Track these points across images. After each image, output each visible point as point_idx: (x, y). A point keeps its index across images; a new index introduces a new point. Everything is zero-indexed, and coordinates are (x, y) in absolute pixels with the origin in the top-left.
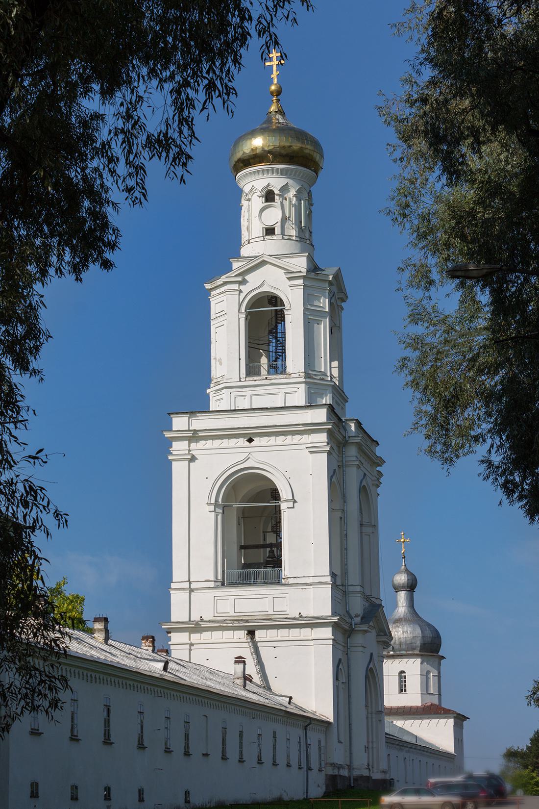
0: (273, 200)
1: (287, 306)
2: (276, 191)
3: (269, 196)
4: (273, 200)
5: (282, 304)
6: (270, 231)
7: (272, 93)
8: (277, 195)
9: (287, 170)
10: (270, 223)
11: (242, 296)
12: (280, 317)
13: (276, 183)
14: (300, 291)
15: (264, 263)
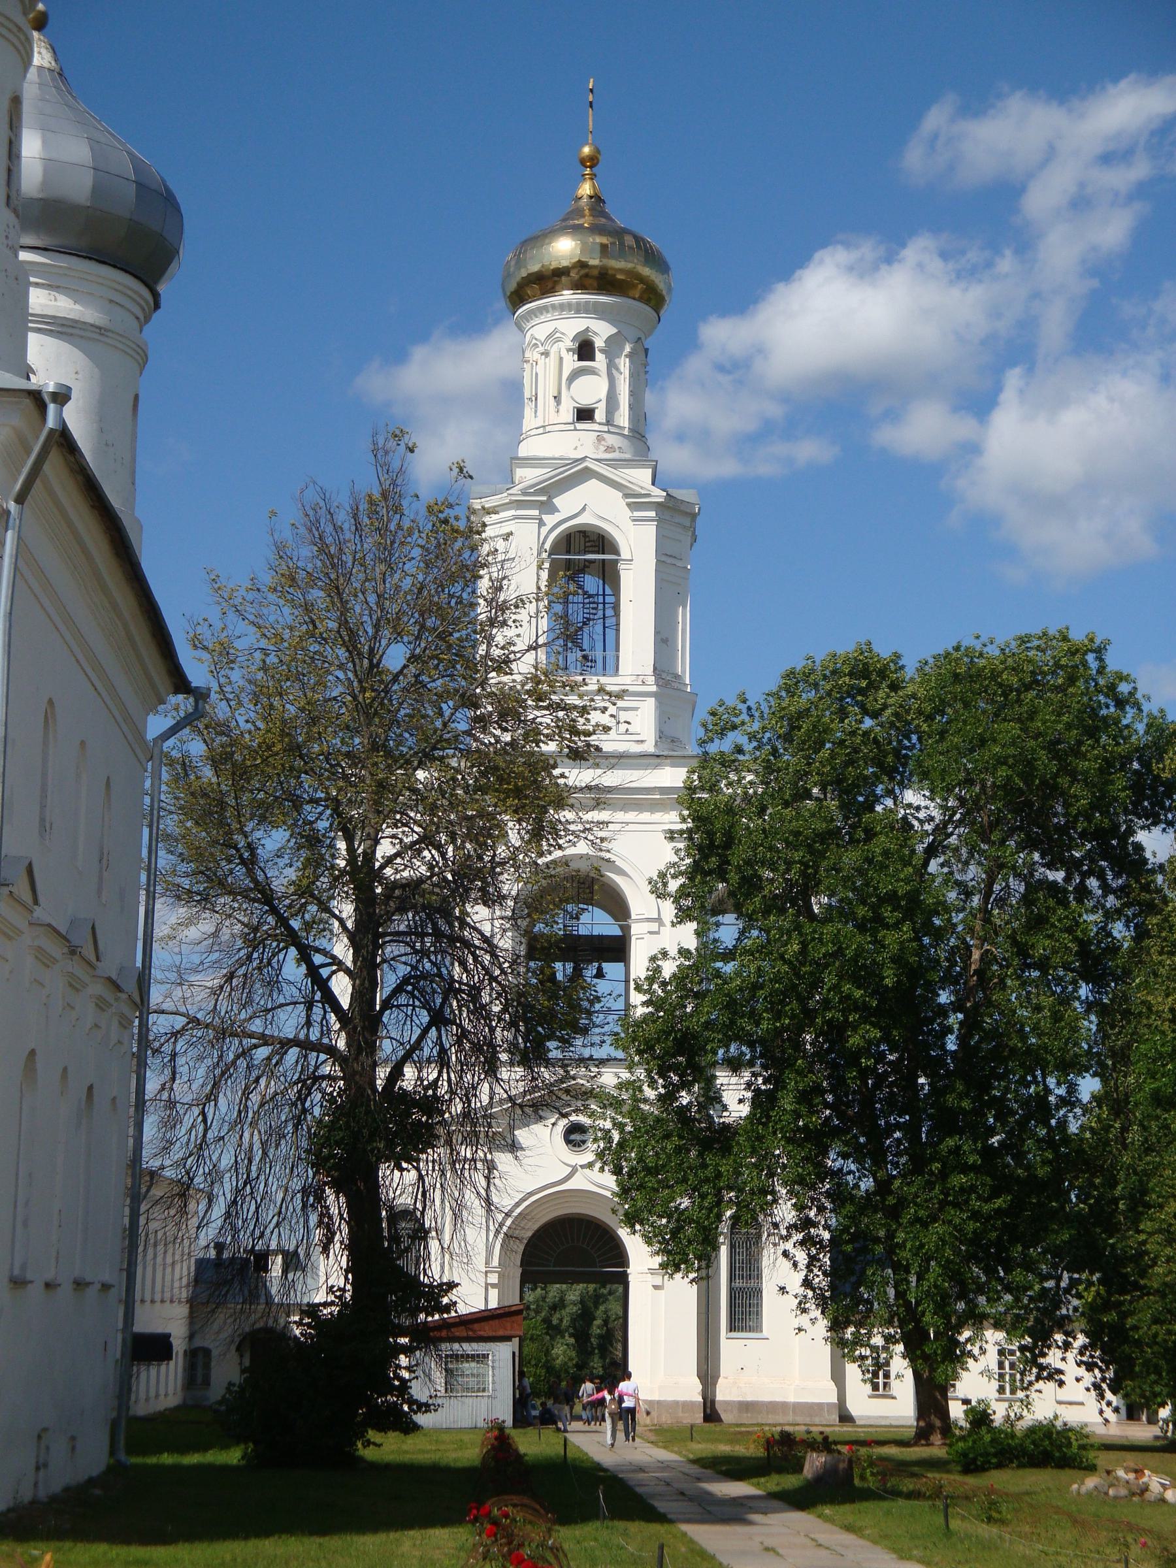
0: (592, 358)
1: (625, 554)
2: (599, 343)
3: (585, 350)
4: (592, 358)
5: (617, 553)
6: (584, 414)
7: (583, 162)
8: (601, 351)
9: (596, 303)
10: (585, 401)
11: (544, 531)
12: (609, 574)
13: (602, 331)
14: (650, 530)
15: (586, 474)
